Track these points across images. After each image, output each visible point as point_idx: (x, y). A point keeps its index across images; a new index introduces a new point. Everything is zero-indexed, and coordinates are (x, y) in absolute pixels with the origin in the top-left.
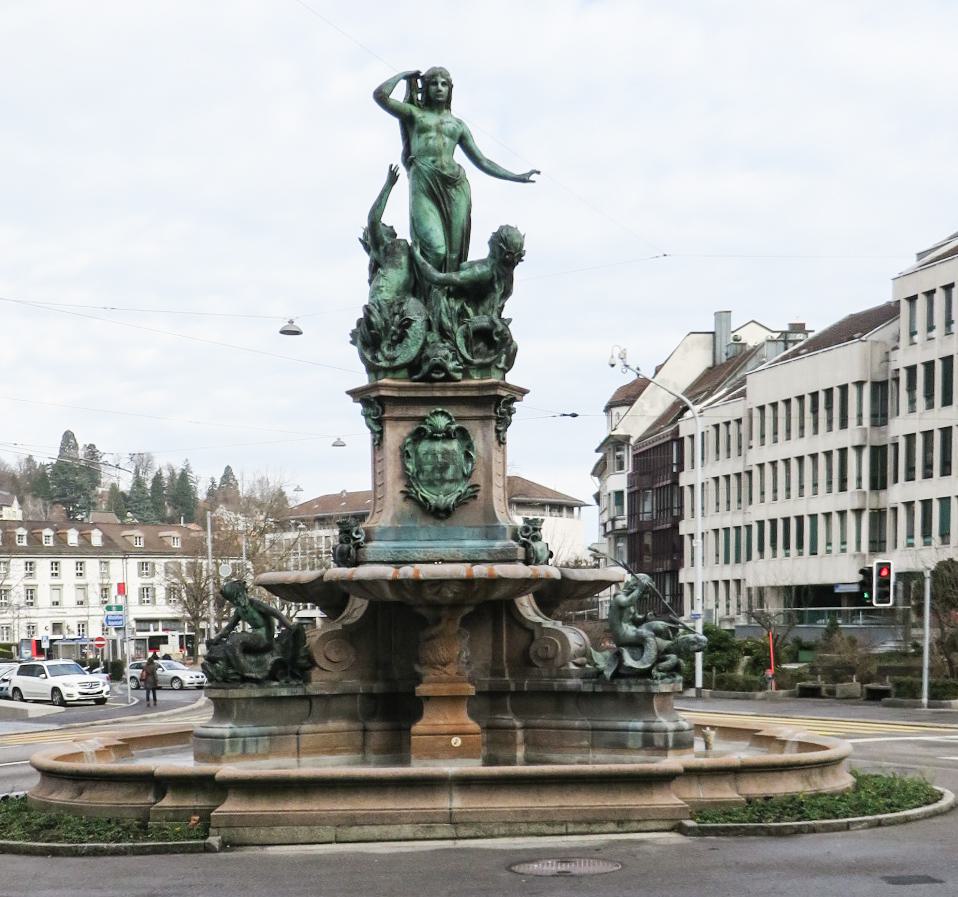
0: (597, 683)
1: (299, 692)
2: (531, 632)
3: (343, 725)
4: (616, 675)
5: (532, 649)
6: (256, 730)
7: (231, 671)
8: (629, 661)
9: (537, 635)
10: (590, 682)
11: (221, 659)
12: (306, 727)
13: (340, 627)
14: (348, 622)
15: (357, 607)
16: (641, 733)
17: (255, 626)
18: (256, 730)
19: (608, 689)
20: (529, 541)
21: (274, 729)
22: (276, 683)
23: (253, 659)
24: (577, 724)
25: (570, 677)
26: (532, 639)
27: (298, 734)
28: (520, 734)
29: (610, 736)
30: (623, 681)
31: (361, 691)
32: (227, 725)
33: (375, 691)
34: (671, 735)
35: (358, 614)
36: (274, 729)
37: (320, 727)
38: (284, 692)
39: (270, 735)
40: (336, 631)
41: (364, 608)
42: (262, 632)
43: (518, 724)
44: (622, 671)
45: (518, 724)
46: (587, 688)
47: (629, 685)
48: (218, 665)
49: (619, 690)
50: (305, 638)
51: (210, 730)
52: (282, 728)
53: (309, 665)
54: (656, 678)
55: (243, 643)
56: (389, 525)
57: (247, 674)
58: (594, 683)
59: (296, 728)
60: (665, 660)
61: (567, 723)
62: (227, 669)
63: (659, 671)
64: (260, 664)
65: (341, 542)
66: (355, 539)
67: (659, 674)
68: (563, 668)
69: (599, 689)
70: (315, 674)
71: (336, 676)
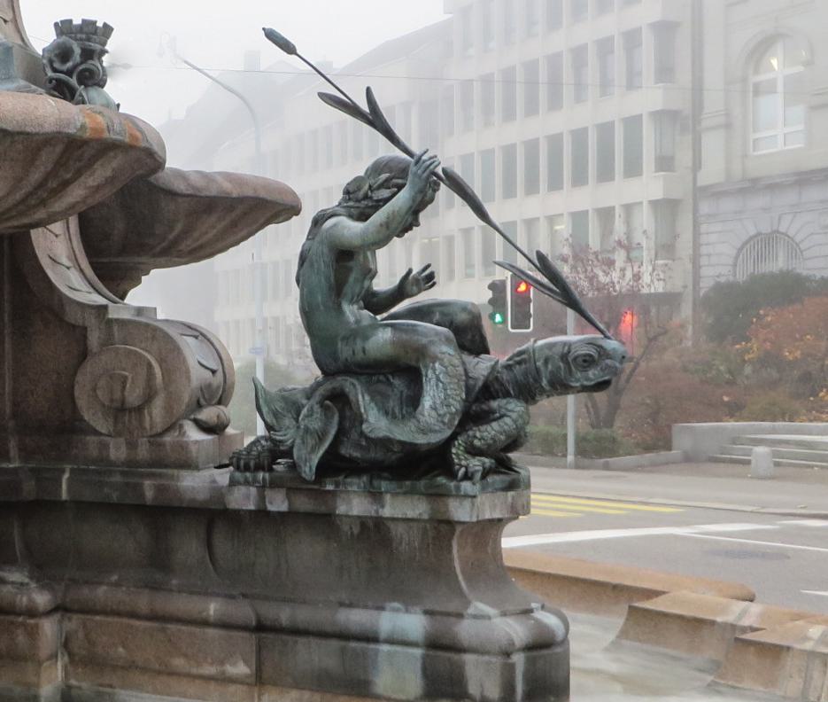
0: (275, 484)
2: (81, 333)
4: (334, 465)
5: (83, 380)
8: (376, 423)
9: (94, 339)
10: (247, 483)
16: (418, 652)
19: (304, 504)
20: (73, 81)
24: (213, 608)
25: (189, 465)
26: (84, 355)
28: (48, 627)
29: (316, 655)
30: (356, 484)
34: (519, 660)
43: (42, 599)
44: (347, 450)
45: (42, 599)
46: (243, 499)
47: (376, 496)
49: (341, 509)
54: (468, 477)
58: (262, 488)
60: (484, 417)
61: (182, 604)
63: (473, 451)
67: (476, 464)
68: (168, 439)
69: (278, 503)
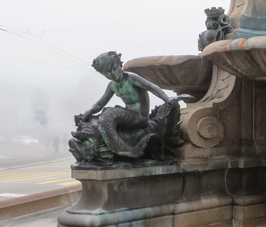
1: (174, 169)
3: (214, 201)
6: (130, 214)
7: (103, 149)
11: (91, 136)
12: (182, 206)
13: (209, 105)
14: (216, 101)
15: (223, 86)
17: (129, 102)
18: (130, 214)
21: (149, 210)
22: (150, 162)
23: (127, 136)
27: (173, 214)
31: (230, 167)
32: (98, 211)
33: (241, 166)
35: (226, 94)
36: (149, 210)
37: (194, 205)
38: (159, 170)
39: (145, 218)
40: (207, 108)
41: (231, 88)
42: (137, 106)
48: (87, 142)
50: (180, 115)
51: (77, 216)
52: (157, 210)
53: (181, 141)
55: (116, 120)
56: (250, 16)
57: (121, 153)
59: (171, 207)
62: (98, 147)
64: (134, 142)
65: (209, 28)
66: (222, 25)
70: (188, 150)
71: (206, 152)
